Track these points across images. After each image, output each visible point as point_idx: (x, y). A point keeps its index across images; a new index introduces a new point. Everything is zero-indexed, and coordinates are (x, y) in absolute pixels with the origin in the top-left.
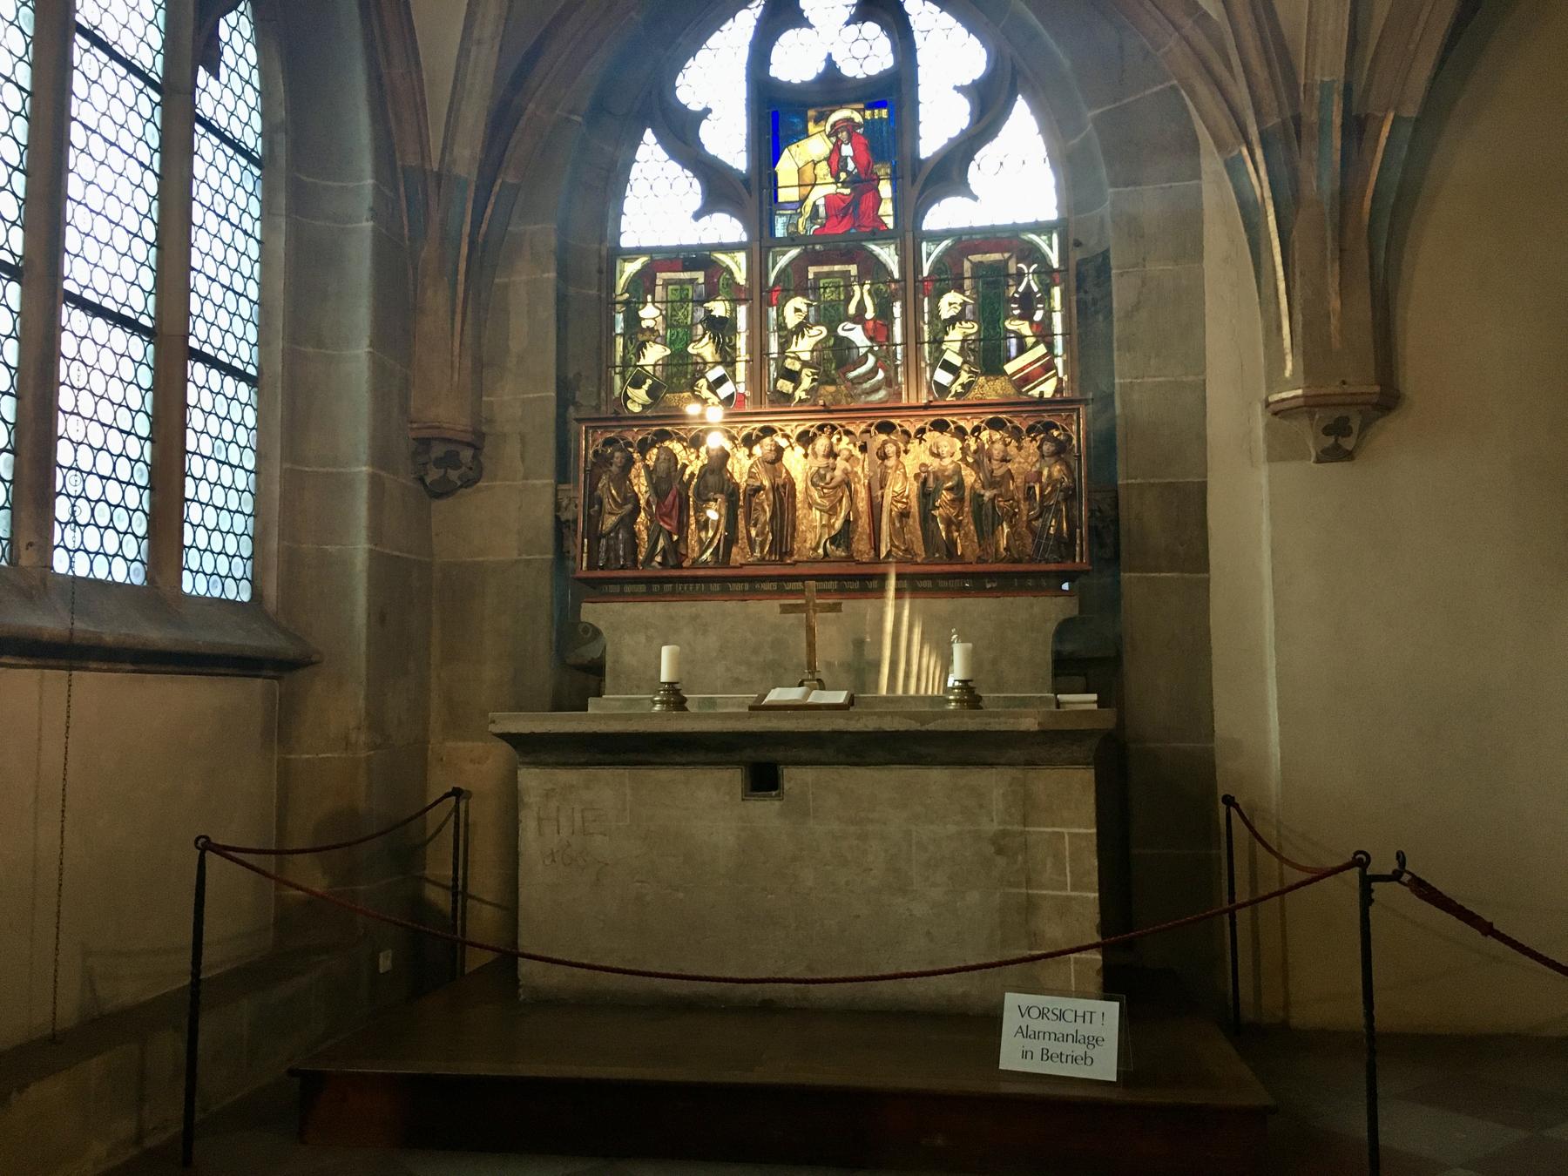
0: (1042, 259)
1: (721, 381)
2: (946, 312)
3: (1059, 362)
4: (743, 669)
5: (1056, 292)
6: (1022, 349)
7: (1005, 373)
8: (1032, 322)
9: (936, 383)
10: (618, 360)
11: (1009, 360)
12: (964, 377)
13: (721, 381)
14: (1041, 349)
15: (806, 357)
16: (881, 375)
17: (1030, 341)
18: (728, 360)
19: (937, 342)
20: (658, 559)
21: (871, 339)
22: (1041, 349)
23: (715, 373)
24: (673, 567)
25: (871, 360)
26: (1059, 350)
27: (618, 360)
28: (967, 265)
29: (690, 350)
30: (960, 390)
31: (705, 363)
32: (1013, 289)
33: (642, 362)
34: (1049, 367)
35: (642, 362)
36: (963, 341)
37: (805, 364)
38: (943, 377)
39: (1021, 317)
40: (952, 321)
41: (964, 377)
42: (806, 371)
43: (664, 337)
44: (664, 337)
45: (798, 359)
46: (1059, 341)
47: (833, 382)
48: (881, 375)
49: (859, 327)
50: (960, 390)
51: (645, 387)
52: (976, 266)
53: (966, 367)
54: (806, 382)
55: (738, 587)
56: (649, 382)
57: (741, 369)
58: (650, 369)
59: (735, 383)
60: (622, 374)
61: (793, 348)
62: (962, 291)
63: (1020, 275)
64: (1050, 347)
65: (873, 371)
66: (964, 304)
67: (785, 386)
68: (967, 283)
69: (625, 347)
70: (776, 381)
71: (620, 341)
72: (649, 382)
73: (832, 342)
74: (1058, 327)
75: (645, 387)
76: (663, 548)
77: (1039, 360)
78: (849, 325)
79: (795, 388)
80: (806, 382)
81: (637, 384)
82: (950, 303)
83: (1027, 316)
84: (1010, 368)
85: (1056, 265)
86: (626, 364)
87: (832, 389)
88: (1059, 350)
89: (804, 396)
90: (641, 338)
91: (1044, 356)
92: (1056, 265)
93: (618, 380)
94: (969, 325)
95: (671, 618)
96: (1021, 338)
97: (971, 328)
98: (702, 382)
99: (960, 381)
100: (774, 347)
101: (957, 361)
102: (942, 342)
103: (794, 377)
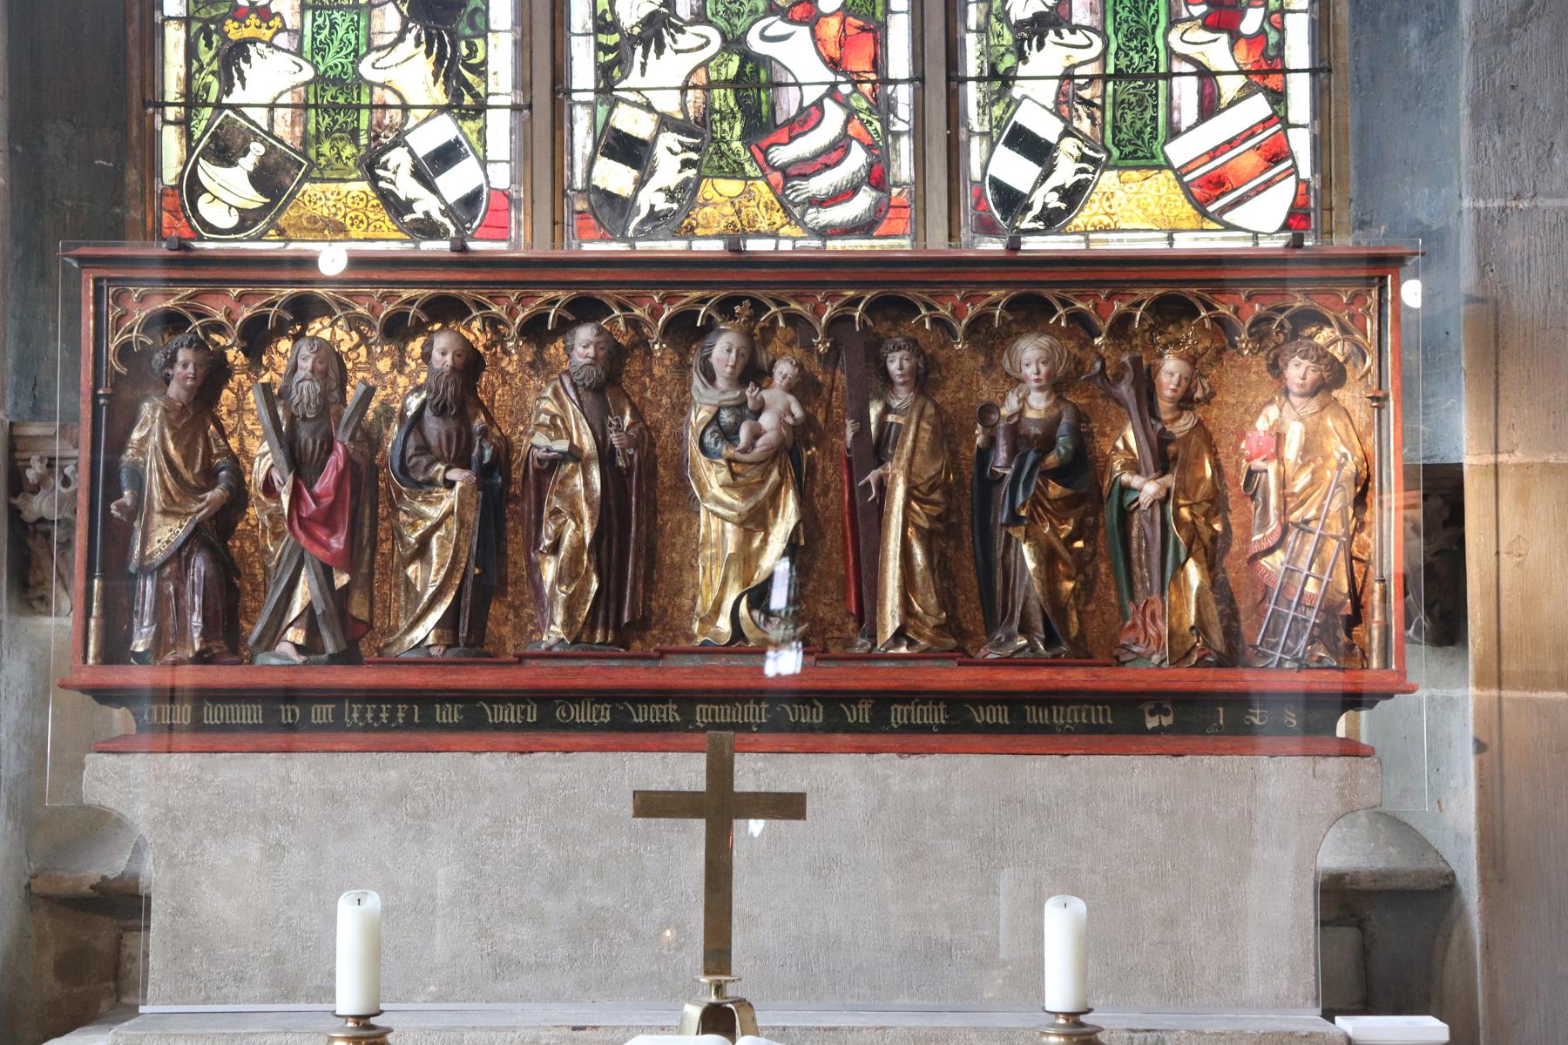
1: (447, 156)
4: (525, 932)
6: (1209, 107)
7: (1169, 166)
8: (1235, 37)
9: (997, 185)
10: (173, 89)
11: (1174, 133)
12: (1066, 172)
13: (447, 156)
14: (1258, 107)
15: (669, 103)
16: (857, 158)
17: (1230, 86)
18: (465, 102)
19: (1000, 80)
20: (296, 635)
21: (833, 64)
23: (430, 135)
24: (334, 660)
25: (834, 117)
27: (173, 89)
29: (365, 69)
30: (1054, 201)
31: (405, 108)
33: (237, 96)
34: (1277, 154)
35: (237, 96)
37: (665, 122)
42: (669, 139)
43: (299, 33)
44: (299, 33)
45: (649, 108)
46: (1299, 91)
47: (737, 172)
48: (857, 158)
49: (803, 32)
50: (1054, 201)
51: (248, 163)
53: (1069, 145)
54: (668, 169)
55: (508, 714)
56: (257, 149)
57: (499, 124)
58: (260, 116)
59: (484, 163)
60: (185, 123)
61: (634, 79)
65: (837, 150)
67: (615, 176)
69: (191, 52)
70: (591, 163)
71: (175, 37)
72: (257, 149)
73: (733, 67)
74: (1298, 52)
75: (248, 163)
76: (309, 609)
77: (1251, 133)
78: (778, 27)
79: (640, 184)
80: (668, 169)
81: (224, 151)
84: (1179, 152)
86: (191, 101)
87: (733, 187)
89: (661, 204)
90: (234, 31)
91: (1266, 123)
93: (172, 145)
94: (1079, 38)
95: (332, 797)
96: (1205, 75)
98: (398, 157)
99: (1054, 180)
100: (583, 74)
101: (1047, 127)
102: (1008, 79)
103: (631, 151)
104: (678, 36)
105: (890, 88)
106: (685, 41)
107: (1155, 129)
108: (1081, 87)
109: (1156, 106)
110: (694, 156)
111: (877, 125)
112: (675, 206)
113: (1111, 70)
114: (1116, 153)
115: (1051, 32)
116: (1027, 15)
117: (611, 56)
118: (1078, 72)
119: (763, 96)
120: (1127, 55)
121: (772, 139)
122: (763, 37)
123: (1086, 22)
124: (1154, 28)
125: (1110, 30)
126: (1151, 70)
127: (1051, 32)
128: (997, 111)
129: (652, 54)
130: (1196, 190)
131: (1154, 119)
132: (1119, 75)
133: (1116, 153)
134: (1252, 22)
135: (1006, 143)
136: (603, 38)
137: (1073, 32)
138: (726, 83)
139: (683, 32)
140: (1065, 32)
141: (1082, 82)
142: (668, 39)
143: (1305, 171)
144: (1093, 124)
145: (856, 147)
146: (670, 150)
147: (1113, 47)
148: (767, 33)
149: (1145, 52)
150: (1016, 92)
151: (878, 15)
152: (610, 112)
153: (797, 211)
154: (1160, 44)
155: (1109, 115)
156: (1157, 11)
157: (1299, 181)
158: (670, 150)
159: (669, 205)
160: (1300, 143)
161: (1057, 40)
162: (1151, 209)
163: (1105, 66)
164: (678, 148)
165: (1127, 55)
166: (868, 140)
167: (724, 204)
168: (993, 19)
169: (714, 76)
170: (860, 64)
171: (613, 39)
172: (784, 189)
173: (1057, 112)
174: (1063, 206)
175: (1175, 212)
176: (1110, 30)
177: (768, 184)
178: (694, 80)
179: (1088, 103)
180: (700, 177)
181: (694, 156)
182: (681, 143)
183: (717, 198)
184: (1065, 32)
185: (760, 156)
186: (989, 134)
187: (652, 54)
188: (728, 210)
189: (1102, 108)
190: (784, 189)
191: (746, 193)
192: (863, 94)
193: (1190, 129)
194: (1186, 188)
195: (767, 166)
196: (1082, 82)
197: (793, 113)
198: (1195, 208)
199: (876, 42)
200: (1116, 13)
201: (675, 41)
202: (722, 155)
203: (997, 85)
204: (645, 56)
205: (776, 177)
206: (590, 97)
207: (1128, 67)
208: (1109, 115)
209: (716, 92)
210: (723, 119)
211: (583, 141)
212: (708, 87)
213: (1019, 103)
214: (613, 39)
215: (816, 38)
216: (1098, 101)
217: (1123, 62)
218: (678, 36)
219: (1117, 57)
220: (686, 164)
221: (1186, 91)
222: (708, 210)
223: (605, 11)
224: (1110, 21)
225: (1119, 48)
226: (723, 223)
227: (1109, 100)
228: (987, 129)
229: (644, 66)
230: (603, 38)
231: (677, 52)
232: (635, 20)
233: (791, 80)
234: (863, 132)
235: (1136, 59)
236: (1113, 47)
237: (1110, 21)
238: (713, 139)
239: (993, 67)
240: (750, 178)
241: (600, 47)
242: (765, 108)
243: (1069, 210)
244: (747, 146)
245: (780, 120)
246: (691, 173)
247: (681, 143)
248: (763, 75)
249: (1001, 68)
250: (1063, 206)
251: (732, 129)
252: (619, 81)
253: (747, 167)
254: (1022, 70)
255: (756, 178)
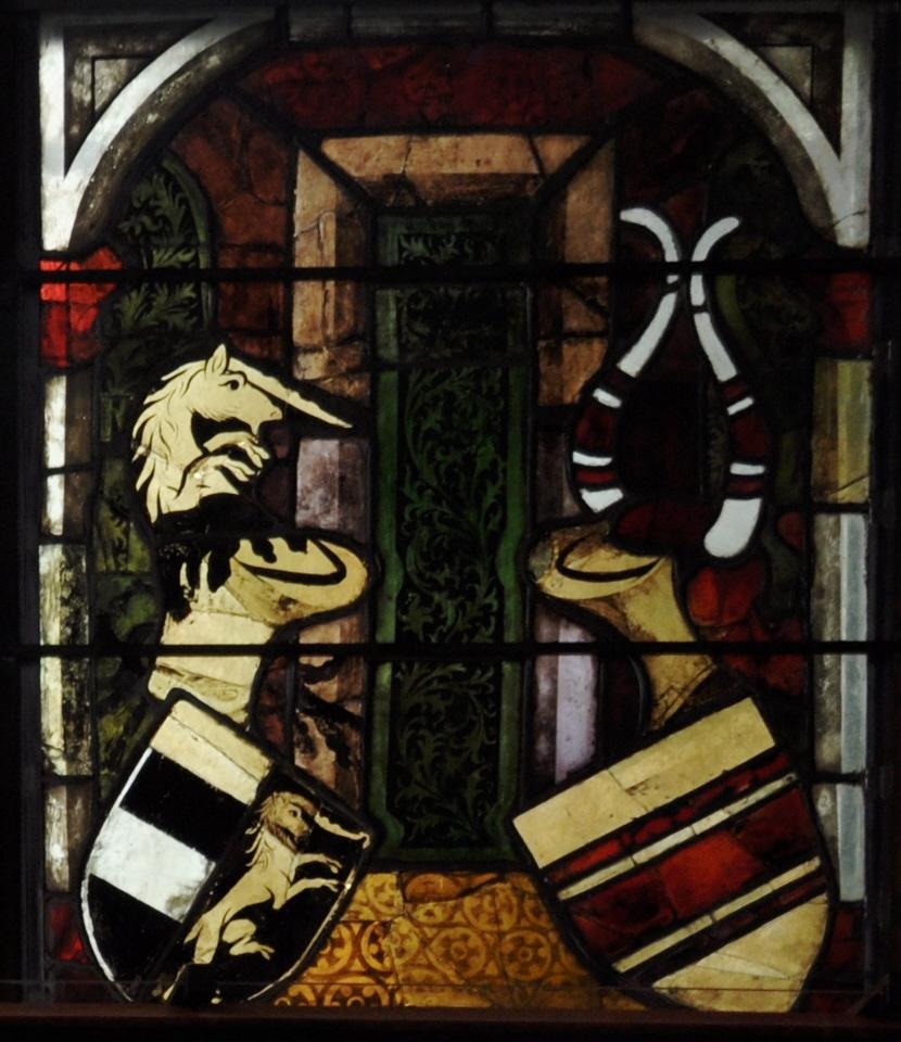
0: (775, 188)
2: (176, 478)
3: (843, 811)
5: (851, 387)
6: (625, 726)
8: (692, 566)
9: (110, 900)
11: (541, 783)
12: (275, 871)
14: (740, 734)
17: (674, 675)
22: (740, 734)
26: (846, 741)
28: (313, 196)
30: (243, 939)
32: (583, 359)
36: (281, 651)
38: (146, 863)
39: (618, 530)
40: (212, 533)
41: (275, 871)
52: (366, 204)
53: (285, 810)
62: (281, 366)
63: (634, 275)
64: (798, 718)
66: (286, 432)
68: (310, 306)
82: (194, 423)
83: (663, 524)
84: (548, 829)
85: (852, 230)
88: (846, 741)
92: (852, 230)
94: (313, 560)
96: (619, 654)
97: (327, 582)
101: (229, 767)
102: (144, 650)
107: (492, 775)
108: (316, 675)
109: (494, 724)
113: (388, 633)
114: (395, 830)
115: (246, 545)
116: (188, 502)
118: (310, 637)
120: (426, 601)
123: (330, 521)
124: (495, 539)
125: (388, 541)
126: (485, 635)
127: (246, 545)
128: (112, 728)
130: (584, 921)
131: (490, 753)
132: (405, 649)
133: (395, 830)
134: (732, 529)
135: (131, 805)
137: (297, 545)
140: (279, 545)
141: (318, 661)
143: (853, 886)
144: (342, 761)
147: (394, 582)
149: (472, 595)
150: (159, 685)
154: (507, 576)
155: (380, 740)
156: (502, 499)
157: (837, 908)
160: (843, 811)
161: (259, 561)
162: (477, 963)
163: (374, 624)
165: (426, 601)
168: (105, 513)
173: (252, 730)
174: (267, 952)
175: (535, 972)
176: (388, 541)
179: (329, 713)
184: (279, 545)
186: (94, 778)
189: (365, 725)
193: (578, 775)
194: (564, 916)
196: (318, 661)
198: (581, 961)
200: (402, 501)
203: (111, 667)
207: (428, 628)
208: (380, 740)
213: (163, 709)
216: (355, 708)
217: (418, 619)
219: (402, 606)
221: (573, 681)
224: (387, 518)
225: (407, 584)
227: (382, 706)
228: (85, 769)
235: (450, 612)
236: (394, 582)
237: (387, 518)
239: (103, 624)
243: (282, 960)
249: (124, 626)
250: (267, 952)
254: (175, 633)
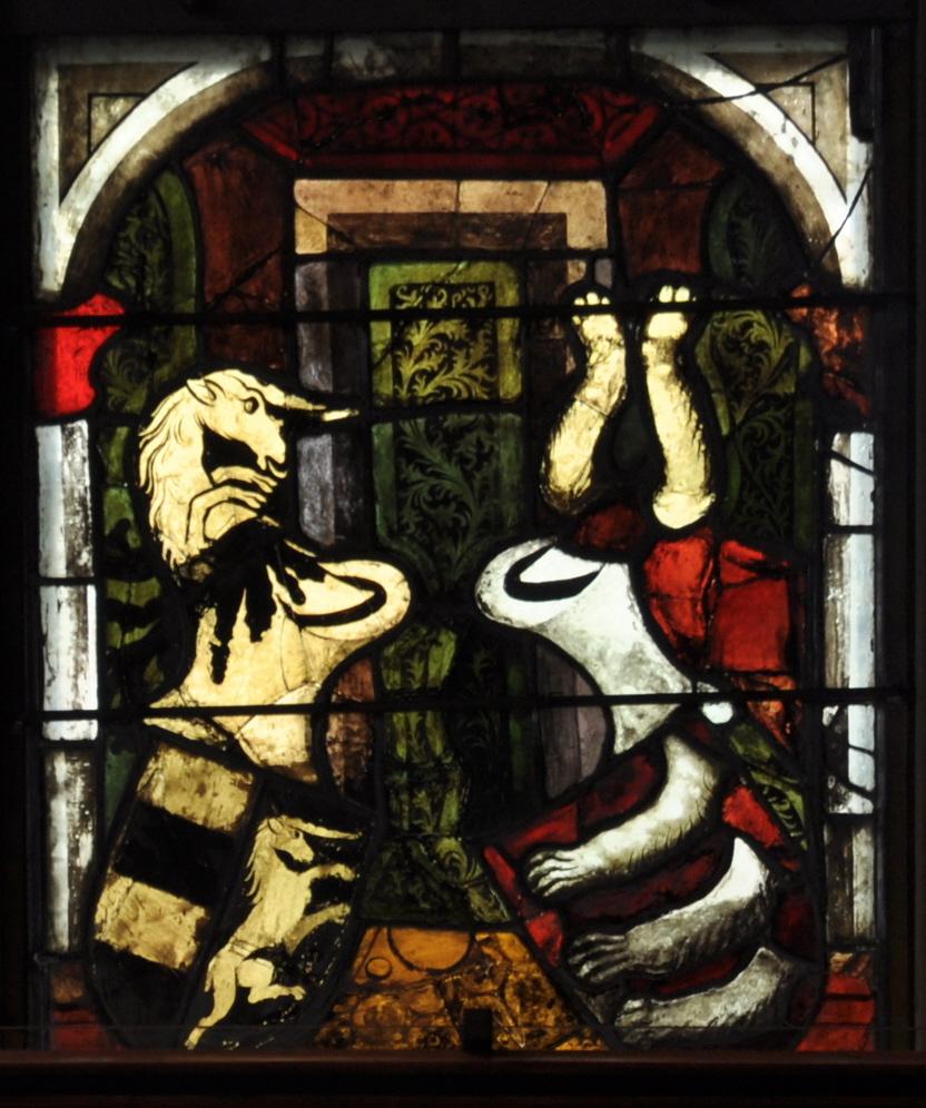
15: (279, 741)
16: (744, 876)
37: (272, 791)
47: (448, 913)
61: (198, 687)
65: (692, 860)
67: (149, 919)
70: (90, 887)
73: (442, 659)
78: (555, 565)
79: (212, 939)
80: (281, 905)
87: (438, 948)
89: (261, 982)
100: (73, 679)
104: (306, 585)
105: (829, 712)
106: (323, 596)
110: (342, 871)
111: (796, 799)
112: (298, 993)
117: (139, 634)
119: (515, 729)
121: (538, 834)
122: (516, 588)
129: (241, 629)
136: (121, 592)
138: (424, 698)
139: (319, 576)
142: (279, 591)
145: (743, 854)
146: (285, 857)
148: (528, 576)
151: (801, 534)
152: (139, 768)
153: (595, 1006)
158: (285, 857)
159: (277, 991)
164: (304, 853)
166: (772, 836)
167: (418, 988)
169: (394, 679)
170: (753, 653)
171: (145, 592)
172: (567, 950)
177: (526, 940)
178: (344, 690)
180: (357, 924)
181: (342, 871)
182: (311, 840)
183: (400, 972)
185: (507, 875)
187: (241, 629)
188: (427, 1001)
190: (567, 950)
191: (473, 961)
192: (761, 729)
195: (527, 898)
197: (588, 768)
199: (794, 600)
201: (299, 597)
202: (415, 870)
204: (224, 631)
205: (543, 926)
206: (87, 730)
209: (398, 719)
210: (412, 788)
211: (70, 838)
212: (376, 710)
214: (145, 592)
215: (646, 594)
218: (306, 585)
220: (324, 891)
222: (380, 1001)
223: (123, 525)
226: (416, 1035)
229: (220, 659)
230: (121, 592)
231: (304, 622)
232: (197, 545)
233: (583, 690)
234: (760, 817)
238: (392, 832)
240: (483, 926)
241: (107, 609)
242: (518, 760)
244: (474, 848)
245: (557, 785)
246: (337, 912)
247: (311, 840)
248: (515, 678)
251: (438, 807)
252: (163, 692)
253: (476, 900)
255: (499, 926)
